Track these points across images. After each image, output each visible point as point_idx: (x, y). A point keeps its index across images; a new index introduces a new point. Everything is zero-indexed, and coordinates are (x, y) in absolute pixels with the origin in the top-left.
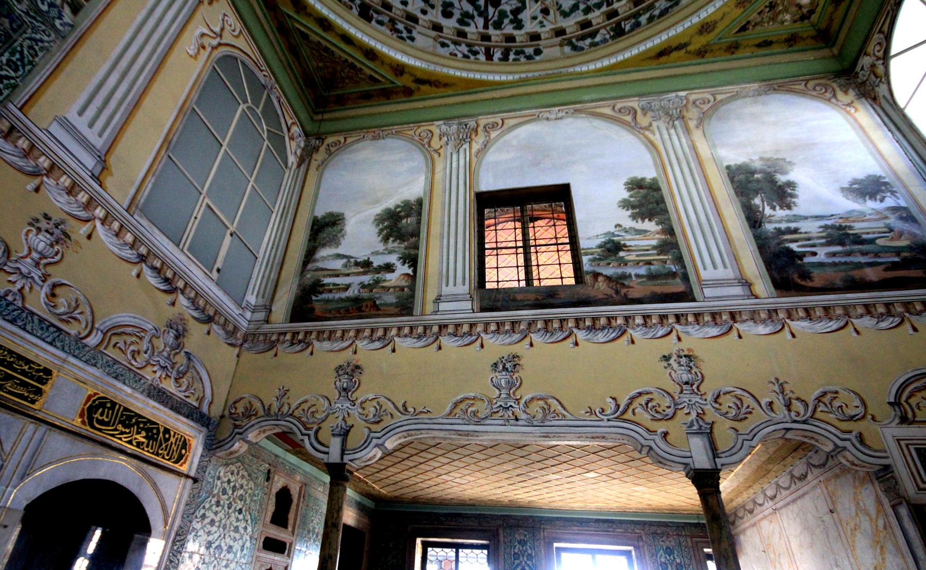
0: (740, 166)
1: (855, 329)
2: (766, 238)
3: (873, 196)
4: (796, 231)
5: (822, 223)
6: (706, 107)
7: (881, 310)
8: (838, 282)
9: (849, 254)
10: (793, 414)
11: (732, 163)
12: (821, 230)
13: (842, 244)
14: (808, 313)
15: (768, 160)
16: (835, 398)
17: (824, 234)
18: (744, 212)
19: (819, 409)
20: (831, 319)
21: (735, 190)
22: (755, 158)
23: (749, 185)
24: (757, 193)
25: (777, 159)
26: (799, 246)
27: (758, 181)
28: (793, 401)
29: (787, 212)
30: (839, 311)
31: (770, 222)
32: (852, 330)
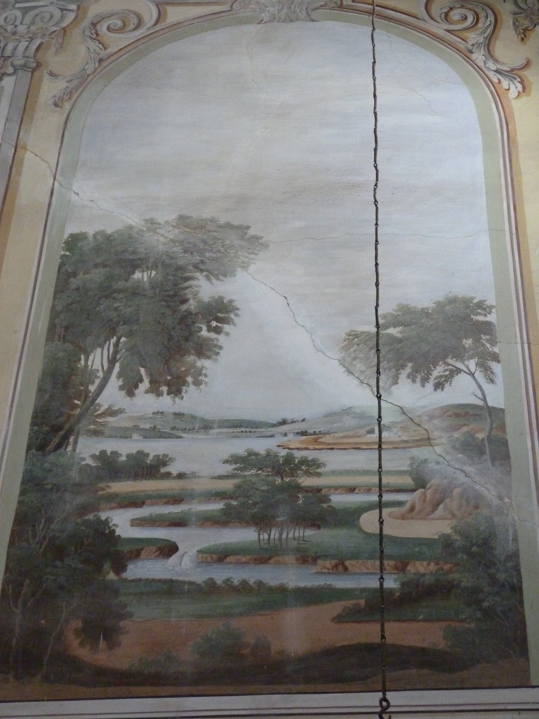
0: (108, 239)
2: (57, 488)
3: (421, 369)
4: (153, 469)
5: (240, 446)
6: (117, 42)
9: (263, 556)
11: (90, 230)
12: (229, 468)
13: (262, 521)
15: (201, 225)
17: (228, 485)
18: (41, 390)
21: (54, 314)
22: (161, 217)
23: (105, 304)
24: (113, 332)
25: (229, 226)
26: (137, 523)
27: (135, 292)
29: (166, 403)
31: (96, 433)
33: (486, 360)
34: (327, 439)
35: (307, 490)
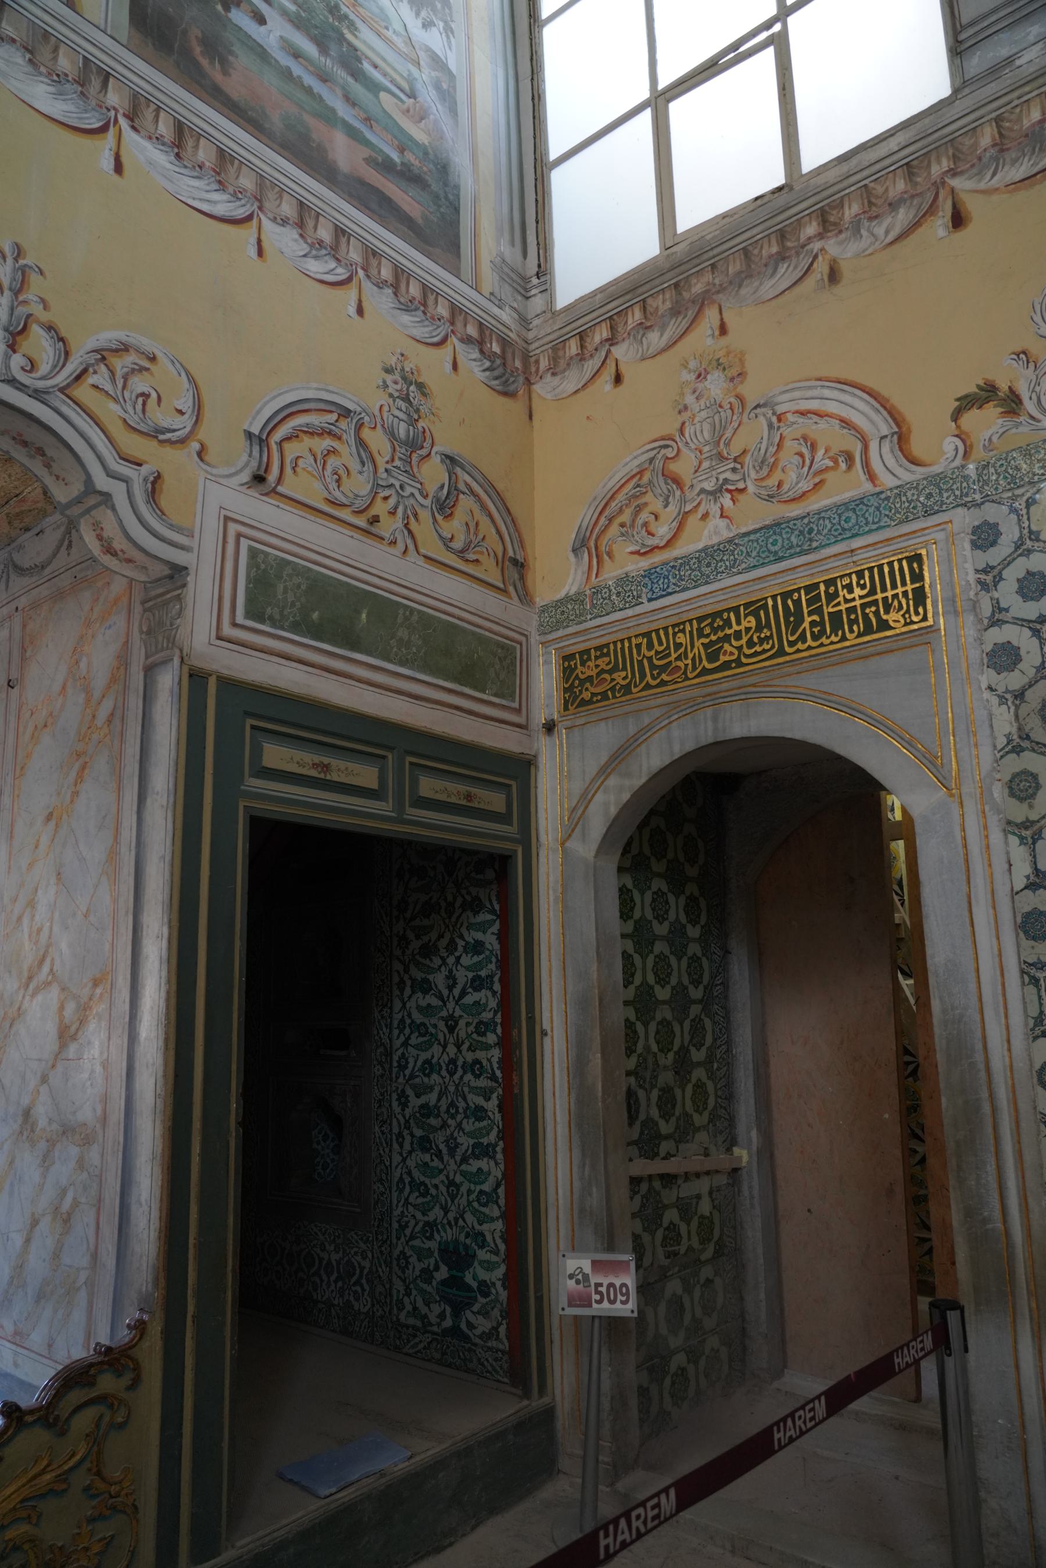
1: (259, 241)
7: (325, 234)
8: (275, 120)
9: (324, 78)
10: (17, 361)
14: (181, 139)
16: (142, 369)
19: (92, 379)
20: (222, 186)
28: (35, 329)
30: (247, 182)
32: (253, 240)
33: (448, 30)
34: (360, 9)
35: (350, 44)
